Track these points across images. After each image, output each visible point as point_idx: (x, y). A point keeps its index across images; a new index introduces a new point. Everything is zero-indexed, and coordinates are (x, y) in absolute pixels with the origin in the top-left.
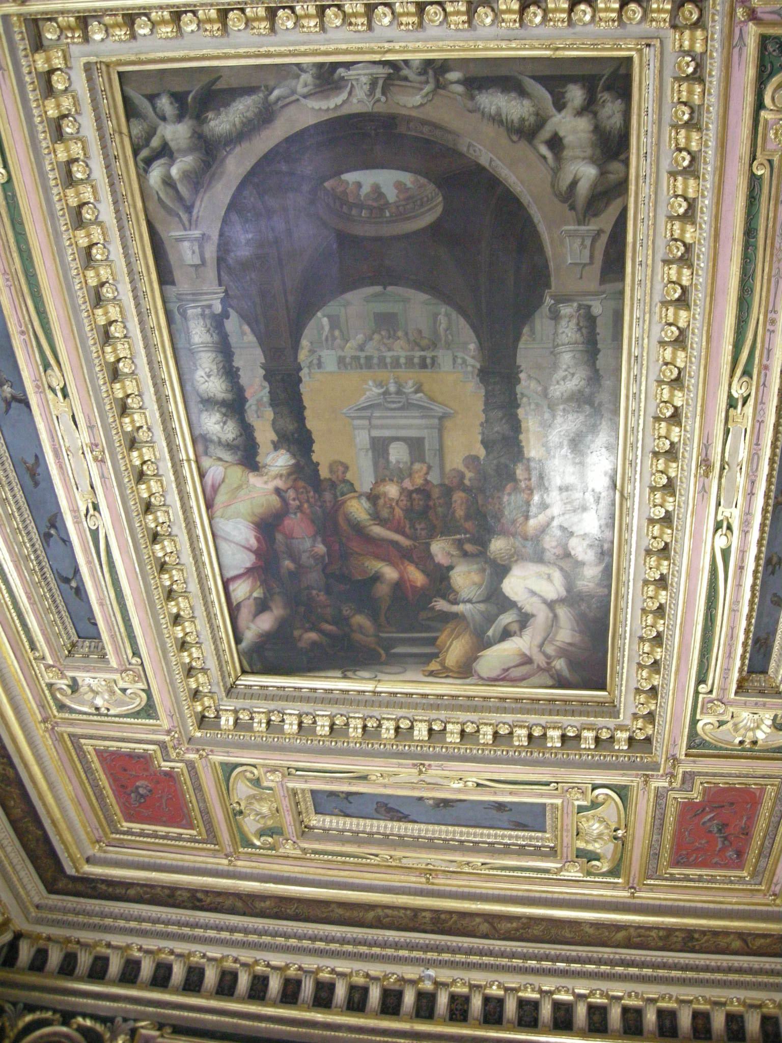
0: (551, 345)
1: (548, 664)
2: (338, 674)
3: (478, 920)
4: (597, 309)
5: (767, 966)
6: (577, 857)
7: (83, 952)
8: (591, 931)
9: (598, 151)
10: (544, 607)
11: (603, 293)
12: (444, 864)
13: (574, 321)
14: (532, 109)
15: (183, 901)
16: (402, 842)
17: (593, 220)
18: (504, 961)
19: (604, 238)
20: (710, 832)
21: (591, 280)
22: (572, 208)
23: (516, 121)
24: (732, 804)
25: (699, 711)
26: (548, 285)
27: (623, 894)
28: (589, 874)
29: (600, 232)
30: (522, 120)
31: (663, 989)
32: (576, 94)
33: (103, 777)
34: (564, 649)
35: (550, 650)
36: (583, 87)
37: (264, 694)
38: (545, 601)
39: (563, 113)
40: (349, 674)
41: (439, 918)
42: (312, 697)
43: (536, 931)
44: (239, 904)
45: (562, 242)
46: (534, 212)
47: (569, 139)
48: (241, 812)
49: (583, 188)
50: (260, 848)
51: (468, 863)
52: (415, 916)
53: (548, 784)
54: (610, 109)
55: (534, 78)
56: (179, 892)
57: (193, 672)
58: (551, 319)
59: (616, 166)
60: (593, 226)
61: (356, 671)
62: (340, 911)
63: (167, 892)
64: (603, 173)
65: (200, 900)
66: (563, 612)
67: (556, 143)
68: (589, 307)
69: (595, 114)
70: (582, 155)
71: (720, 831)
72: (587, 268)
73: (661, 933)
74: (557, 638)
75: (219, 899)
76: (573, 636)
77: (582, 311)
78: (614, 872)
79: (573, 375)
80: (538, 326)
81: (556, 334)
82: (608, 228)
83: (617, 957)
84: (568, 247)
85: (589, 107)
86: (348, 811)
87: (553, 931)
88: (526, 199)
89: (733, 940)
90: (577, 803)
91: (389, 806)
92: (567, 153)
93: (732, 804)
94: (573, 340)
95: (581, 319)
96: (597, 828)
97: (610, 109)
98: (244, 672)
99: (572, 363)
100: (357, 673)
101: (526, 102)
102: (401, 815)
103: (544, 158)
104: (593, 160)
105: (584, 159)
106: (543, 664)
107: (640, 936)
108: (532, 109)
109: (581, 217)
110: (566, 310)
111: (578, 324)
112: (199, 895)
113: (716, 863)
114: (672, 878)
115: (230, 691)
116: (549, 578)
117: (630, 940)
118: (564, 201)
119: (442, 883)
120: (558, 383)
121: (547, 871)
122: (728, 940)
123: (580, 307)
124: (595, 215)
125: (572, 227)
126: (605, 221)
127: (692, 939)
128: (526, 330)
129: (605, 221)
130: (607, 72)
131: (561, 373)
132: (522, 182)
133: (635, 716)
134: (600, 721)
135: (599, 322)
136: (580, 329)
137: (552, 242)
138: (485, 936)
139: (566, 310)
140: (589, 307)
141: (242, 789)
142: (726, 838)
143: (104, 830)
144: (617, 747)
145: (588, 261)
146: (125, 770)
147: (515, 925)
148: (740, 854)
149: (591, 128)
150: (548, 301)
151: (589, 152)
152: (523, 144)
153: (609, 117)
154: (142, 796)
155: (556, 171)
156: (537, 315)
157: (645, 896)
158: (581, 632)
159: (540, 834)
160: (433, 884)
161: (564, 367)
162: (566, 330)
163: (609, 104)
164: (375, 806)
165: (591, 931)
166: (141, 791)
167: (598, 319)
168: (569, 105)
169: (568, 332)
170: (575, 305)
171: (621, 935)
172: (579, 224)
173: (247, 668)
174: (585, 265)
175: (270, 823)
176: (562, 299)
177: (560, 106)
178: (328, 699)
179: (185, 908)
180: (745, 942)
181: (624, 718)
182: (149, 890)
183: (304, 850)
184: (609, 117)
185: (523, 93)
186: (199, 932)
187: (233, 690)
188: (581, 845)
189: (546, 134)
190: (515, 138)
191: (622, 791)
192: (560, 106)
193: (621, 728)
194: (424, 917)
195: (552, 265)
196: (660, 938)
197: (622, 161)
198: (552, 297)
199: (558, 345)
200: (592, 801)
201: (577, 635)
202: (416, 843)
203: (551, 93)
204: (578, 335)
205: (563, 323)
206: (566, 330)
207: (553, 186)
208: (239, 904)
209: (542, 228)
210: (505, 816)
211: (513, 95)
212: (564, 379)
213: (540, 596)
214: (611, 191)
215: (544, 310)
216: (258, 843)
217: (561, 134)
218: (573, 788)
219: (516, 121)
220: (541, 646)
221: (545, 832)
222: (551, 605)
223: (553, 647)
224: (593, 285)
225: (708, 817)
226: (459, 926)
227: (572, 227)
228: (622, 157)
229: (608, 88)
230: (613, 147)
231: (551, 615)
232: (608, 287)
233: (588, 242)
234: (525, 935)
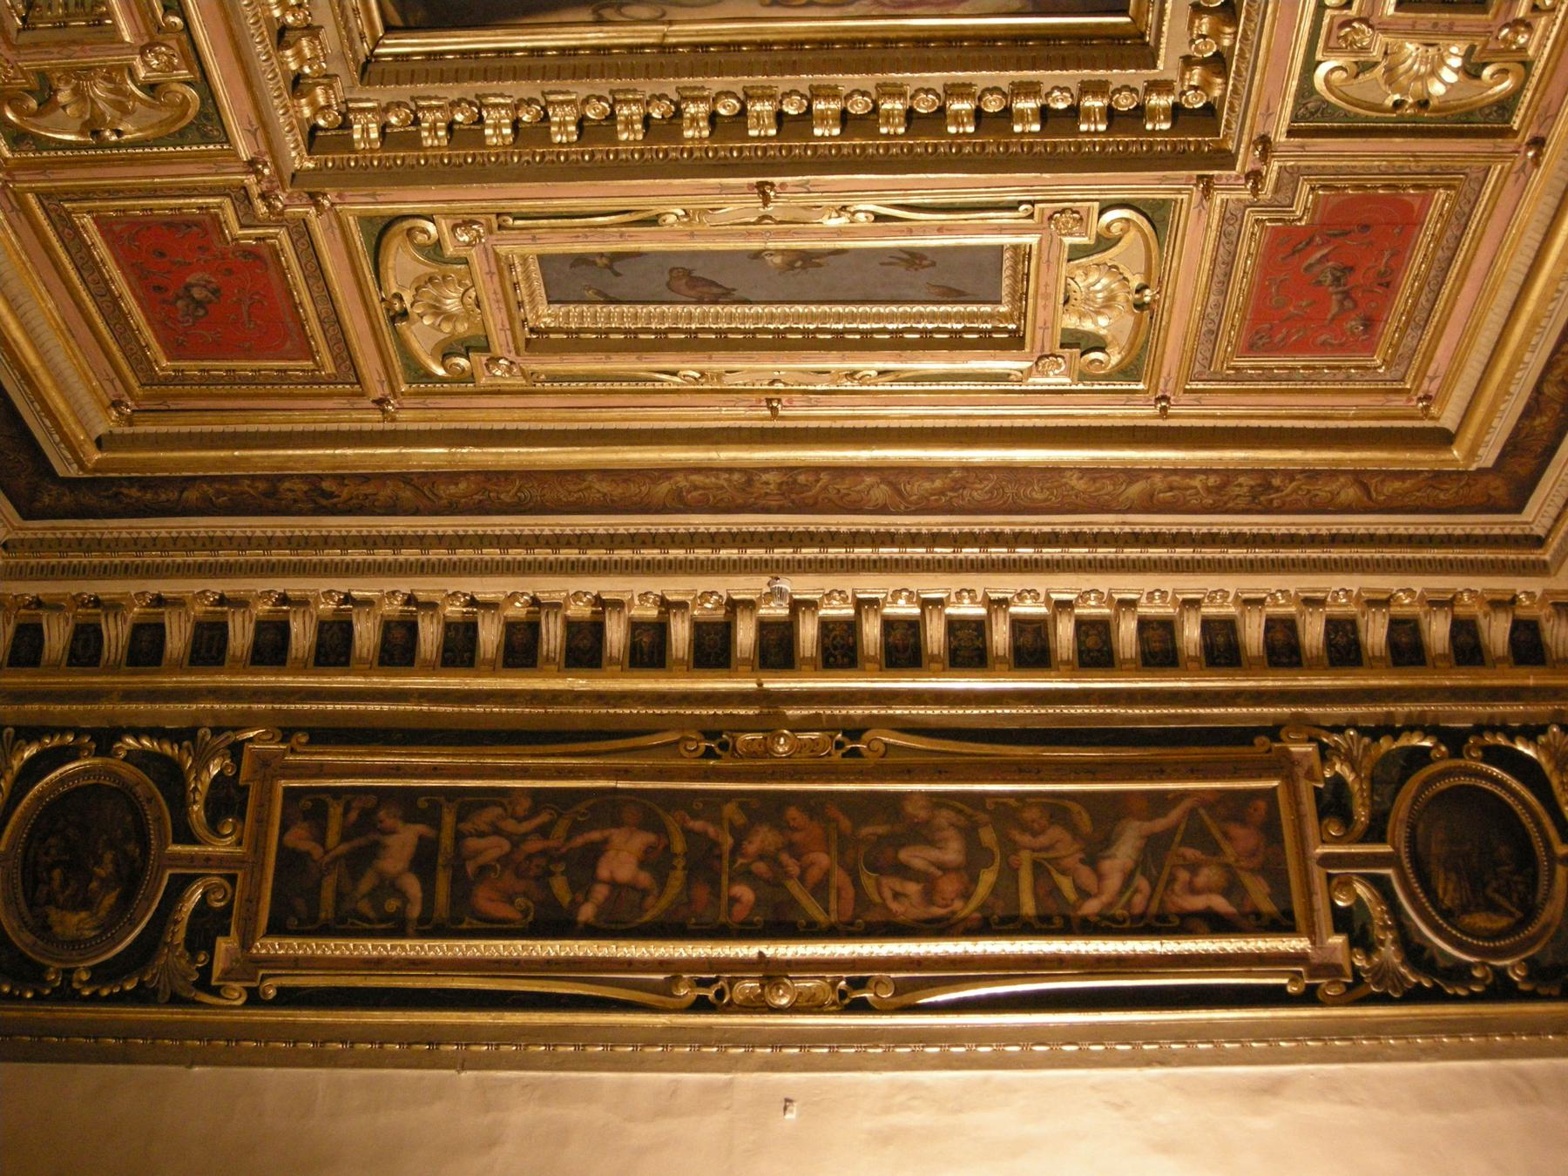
2: (586, 15)
3: (869, 480)
5: (1401, 530)
6: (1062, 346)
7: (111, 620)
8: (1080, 485)
12: (805, 378)
15: (295, 501)
16: (724, 342)
18: (919, 552)
20: (1319, 283)
24: (1366, 227)
25: (1321, 44)
27: (1142, 414)
28: (1083, 377)
31: (1210, 582)
33: (117, 274)
37: (435, 67)
40: (608, 14)
41: (795, 481)
42: (536, 65)
43: (978, 493)
44: (407, 494)
48: (404, 314)
50: (442, 380)
51: (851, 375)
52: (750, 482)
53: (1012, 207)
56: (287, 485)
57: (289, 36)
61: (622, 5)
62: (605, 487)
63: (262, 486)
65: (331, 495)
71: (1337, 280)
73: (1212, 481)
75: (368, 489)
78: (1129, 371)
83: (1127, 529)
86: (612, 294)
87: (1010, 490)
89: (1343, 486)
90: (1068, 240)
91: (695, 274)
93: (1366, 227)
96: (1102, 283)
98: (389, 29)
100: (626, 10)
102: (720, 291)
107: (1171, 489)
112: (325, 485)
113: (1324, 344)
114: (1239, 375)
115: (368, 70)
117: (1152, 496)
119: (796, 413)
121: (1003, 377)
122: (1334, 486)
127: (1267, 487)
133: (1188, 62)
134: (1116, 76)
138: (883, 510)
141: (403, 264)
142: (1347, 295)
143: (124, 381)
144: (1149, 127)
146: (162, 255)
147: (938, 484)
148: (1370, 323)
154: (199, 304)
157: (1185, 414)
159: (987, 308)
160: (783, 418)
164: (667, 277)
165: (1080, 485)
166: (197, 293)
171: (1136, 489)
173: (396, 20)
175: (462, 328)
178: (570, 64)
179: (300, 513)
180: (1365, 488)
181: (1166, 66)
182: (226, 487)
183: (531, 376)
186: (334, 555)
187: (370, 67)
188: (1071, 322)
191: (1156, 214)
193: (1156, 86)
194: (767, 483)
196: (1208, 490)
200: (1098, 236)
202: (752, 343)
208: (407, 494)
210: (923, 276)
216: (440, 372)
218: (1063, 211)
221: (999, 302)
225: (1318, 255)
226: (832, 494)
234: (955, 502)
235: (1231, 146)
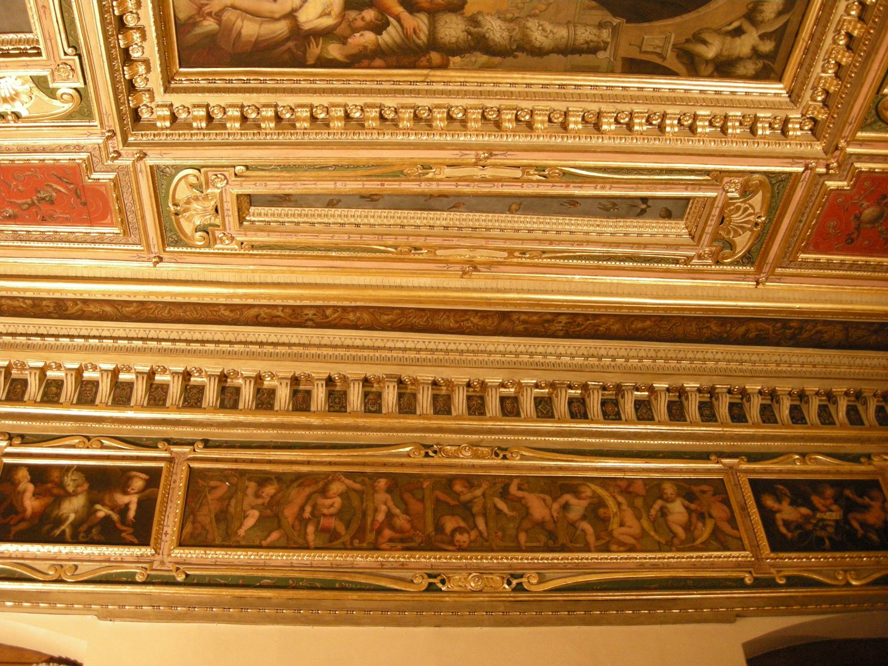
0: (576, 20)
1: (210, 14)
4: (601, 55)
9: (724, 59)
10: (288, 8)
11: (615, 59)
13: (595, 39)
14: (766, 19)
17: (675, 54)
19: (658, 61)
21: (626, 50)
22: (687, 41)
23: (762, 8)
26: (627, 22)
29: (664, 58)
30: (762, 12)
32: (767, 47)
34: (231, 30)
35: (229, 16)
36: (771, 52)
38: (295, 10)
39: (757, 39)
45: (662, 33)
46: (693, 15)
47: (738, 41)
49: (700, 49)
54: (750, 68)
55: (788, 22)
58: (600, 23)
59: (710, 69)
60: (669, 54)
64: (707, 62)
66: (281, 28)
67: (738, 32)
68: (605, 49)
69: (750, 58)
70: (724, 49)
72: (638, 49)
74: (245, 22)
76: (251, 36)
77: (602, 44)
79: (547, 37)
80: (594, 12)
81: (586, 25)
82: (666, 64)
84: (658, 36)
85: (756, 53)
88: (703, 10)
92: (728, 39)
94: (578, 37)
95: (595, 44)
97: (750, 68)
99: (557, 36)
101: (773, 15)
103: (730, 24)
104: (717, 57)
105: (721, 50)
106: (207, 9)
108: (766, 19)
109: (679, 46)
110: (605, 34)
111: (591, 41)
116: (325, 14)
118: (694, 36)
120: (540, 25)
123: (607, 43)
124: (678, 56)
125: (672, 40)
126: (671, 61)
128: (594, 4)
129: (671, 61)
130: (776, 67)
131: (549, 27)
132: (717, 8)
135: (591, 56)
136: (587, 42)
137: (665, 26)
139: (605, 34)
140: (605, 49)
145: (643, 49)
149: (741, 56)
150: (616, 21)
151: (725, 53)
152: (744, 11)
153: (745, 67)
155: (718, 31)
156: (606, 12)
158: (257, 43)
161: (555, 30)
162: (588, 33)
163: (753, 67)
167: (594, 56)
168: (761, 42)
169: (585, 35)
170: (609, 40)
172: (673, 45)
174: (640, 47)
176: (615, 30)
177: (762, 37)
184: (745, 67)
185: (780, 14)
189: (746, 26)
190: (750, 6)
192: (762, 37)
195: (646, 24)
197: (712, 73)
198: (620, 23)
199: (575, 26)
201: (253, 40)
203: (774, 32)
204: (582, 41)
205: (595, 31)
206: (588, 33)
207: (707, 29)
209: (678, 19)
211: (781, 8)
212: (544, 30)
213: (301, 7)
214: (693, 66)
215: (609, 18)
217: (743, 37)
219: (762, 8)
220: (234, 7)
222: (291, 16)
223: (233, 18)
224: (623, 52)
227: (672, 40)
228: (715, 74)
229: (765, 67)
230: (724, 68)
231: (277, 16)
232: (619, 64)
233: (658, 50)
235: (131, 139)
